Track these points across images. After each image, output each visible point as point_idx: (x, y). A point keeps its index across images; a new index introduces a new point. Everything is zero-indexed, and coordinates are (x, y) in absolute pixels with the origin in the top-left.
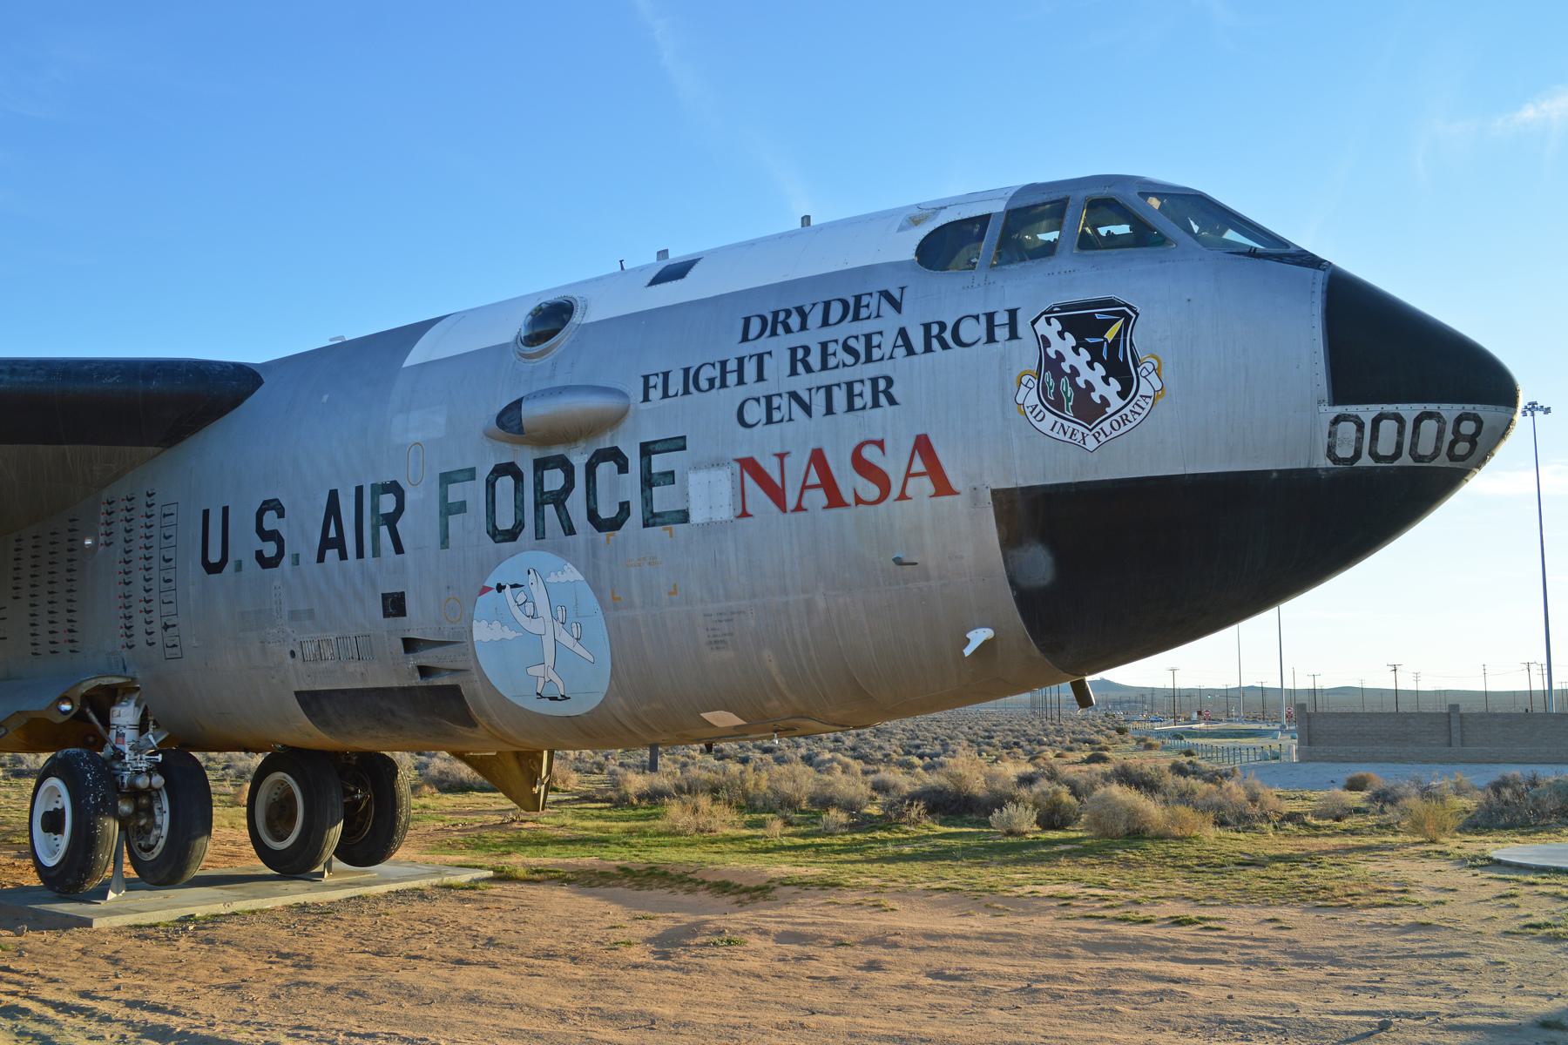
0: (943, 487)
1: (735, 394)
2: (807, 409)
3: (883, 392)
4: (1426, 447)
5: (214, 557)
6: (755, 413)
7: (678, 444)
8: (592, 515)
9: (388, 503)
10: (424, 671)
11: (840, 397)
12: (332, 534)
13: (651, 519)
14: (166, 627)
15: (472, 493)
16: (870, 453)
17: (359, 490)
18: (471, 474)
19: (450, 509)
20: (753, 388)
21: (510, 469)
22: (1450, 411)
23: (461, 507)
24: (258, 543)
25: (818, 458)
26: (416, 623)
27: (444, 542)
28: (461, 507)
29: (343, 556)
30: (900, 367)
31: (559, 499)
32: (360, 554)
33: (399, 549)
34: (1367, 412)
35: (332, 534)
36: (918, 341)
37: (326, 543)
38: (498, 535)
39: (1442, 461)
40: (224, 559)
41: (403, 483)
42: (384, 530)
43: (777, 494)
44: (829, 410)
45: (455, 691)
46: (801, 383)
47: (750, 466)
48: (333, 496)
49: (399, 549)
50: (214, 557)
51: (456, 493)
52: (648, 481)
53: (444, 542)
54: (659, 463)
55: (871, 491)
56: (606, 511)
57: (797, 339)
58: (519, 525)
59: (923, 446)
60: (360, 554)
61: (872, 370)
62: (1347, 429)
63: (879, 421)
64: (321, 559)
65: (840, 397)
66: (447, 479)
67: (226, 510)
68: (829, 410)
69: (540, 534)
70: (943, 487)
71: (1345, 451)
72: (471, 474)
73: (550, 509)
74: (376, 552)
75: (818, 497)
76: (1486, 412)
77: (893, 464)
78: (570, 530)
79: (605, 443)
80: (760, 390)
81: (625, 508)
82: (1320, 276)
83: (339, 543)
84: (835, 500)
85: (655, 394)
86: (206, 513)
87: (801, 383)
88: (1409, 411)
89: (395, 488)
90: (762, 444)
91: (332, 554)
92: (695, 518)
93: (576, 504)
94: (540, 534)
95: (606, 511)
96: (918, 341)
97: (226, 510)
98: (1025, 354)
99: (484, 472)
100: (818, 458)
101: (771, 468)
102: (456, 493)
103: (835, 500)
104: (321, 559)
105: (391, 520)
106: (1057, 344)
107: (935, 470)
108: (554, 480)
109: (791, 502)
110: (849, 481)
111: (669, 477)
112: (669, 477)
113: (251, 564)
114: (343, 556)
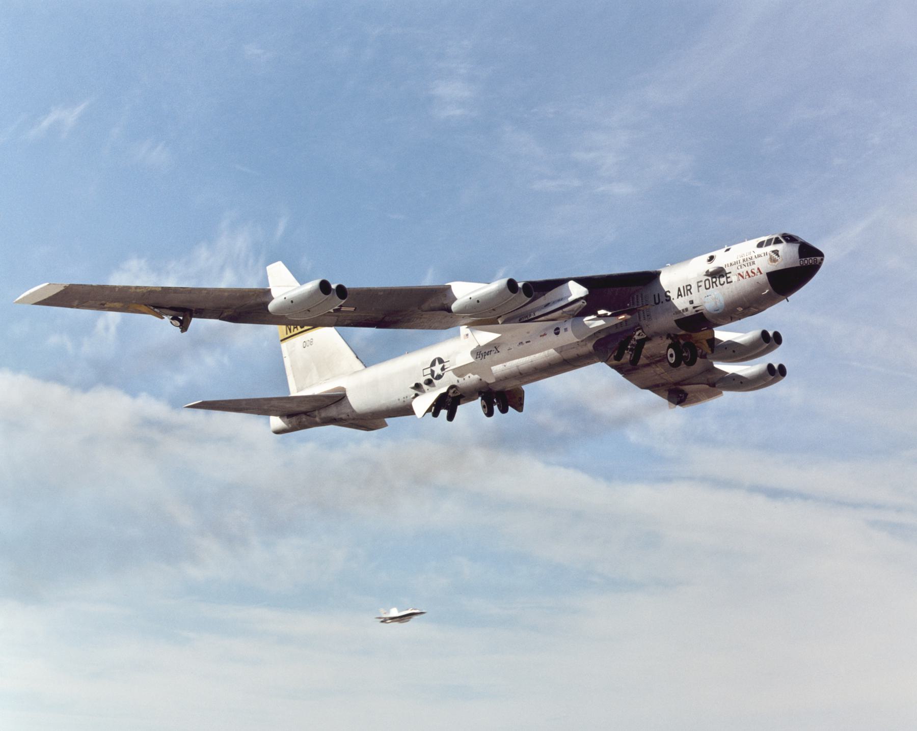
0: (761, 273)
1: (737, 265)
2: (745, 266)
3: (754, 263)
4: (811, 262)
5: (657, 301)
6: (739, 267)
7: (730, 273)
8: (720, 284)
9: (689, 288)
10: (697, 311)
11: (749, 264)
12: (680, 294)
13: (728, 283)
14: (648, 316)
15: (702, 284)
16: (753, 271)
17: (684, 287)
18: (701, 281)
19: (699, 287)
20: (739, 264)
21: (708, 280)
22: (813, 258)
23: (701, 286)
24: (666, 298)
25: (747, 272)
26: (695, 304)
27: (699, 291)
28: (701, 286)
29: (682, 296)
30: (755, 260)
31: (715, 282)
32: (685, 295)
33: (691, 293)
34: (803, 259)
35: (680, 294)
36: (757, 256)
37: (678, 295)
38: (706, 289)
39: (813, 264)
40: (659, 302)
41: (691, 284)
42: (689, 292)
43: (743, 277)
44: (748, 266)
45: (702, 313)
46: (745, 263)
47: (739, 274)
48: (679, 290)
49: (691, 293)
50: (657, 301)
51: (700, 284)
52: (727, 278)
53: (699, 291)
54: (728, 275)
55: (753, 275)
56: (722, 283)
57: (743, 258)
58: (710, 286)
59: (758, 269)
60: (685, 295)
61: (753, 260)
62: (802, 262)
63: (753, 267)
64: (678, 298)
65: (749, 264)
66: (698, 282)
67: (659, 294)
68: (748, 266)
69: (713, 287)
70: (761, 273)
71: (802, 264)
72: (701, 281)
73: (714, 284)
74: (688, 295)
75: (747, 277)
76: (819, 258)
77: (756, 271)
78: (717, 286)
79: (721, 274)
80: (740, 264)
81: (724, 282)
82: (798, 245)
83: (681, 295)
84: (749, 277)
85: (727, 267)
86: (654, 296)
87: (745, 263)
88: (808, 259)
89: (690, 285)
90: (740, 271)
91: (680, 297)
92: (733, 281)
93: (718, 282)
94: (713, 287)
95: (722, 283)
96: (757, 256)
97: (659, 294)
98: (768, 257)
99: (704, 281)
100: (747, 272)
101: (742, 274)
102: (700, 284)
103: (749, 277)
104: (678, 298)
105: (690, 290)
106: (771, 254)
107: (760, 272)
108: (714, 280)
109: (744, 277)
110: (751, 274)
111: (729, 277)
112: (729, 277)
113: (665, 301)
114: (682, 296)
